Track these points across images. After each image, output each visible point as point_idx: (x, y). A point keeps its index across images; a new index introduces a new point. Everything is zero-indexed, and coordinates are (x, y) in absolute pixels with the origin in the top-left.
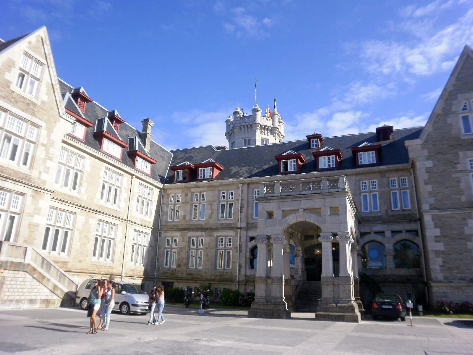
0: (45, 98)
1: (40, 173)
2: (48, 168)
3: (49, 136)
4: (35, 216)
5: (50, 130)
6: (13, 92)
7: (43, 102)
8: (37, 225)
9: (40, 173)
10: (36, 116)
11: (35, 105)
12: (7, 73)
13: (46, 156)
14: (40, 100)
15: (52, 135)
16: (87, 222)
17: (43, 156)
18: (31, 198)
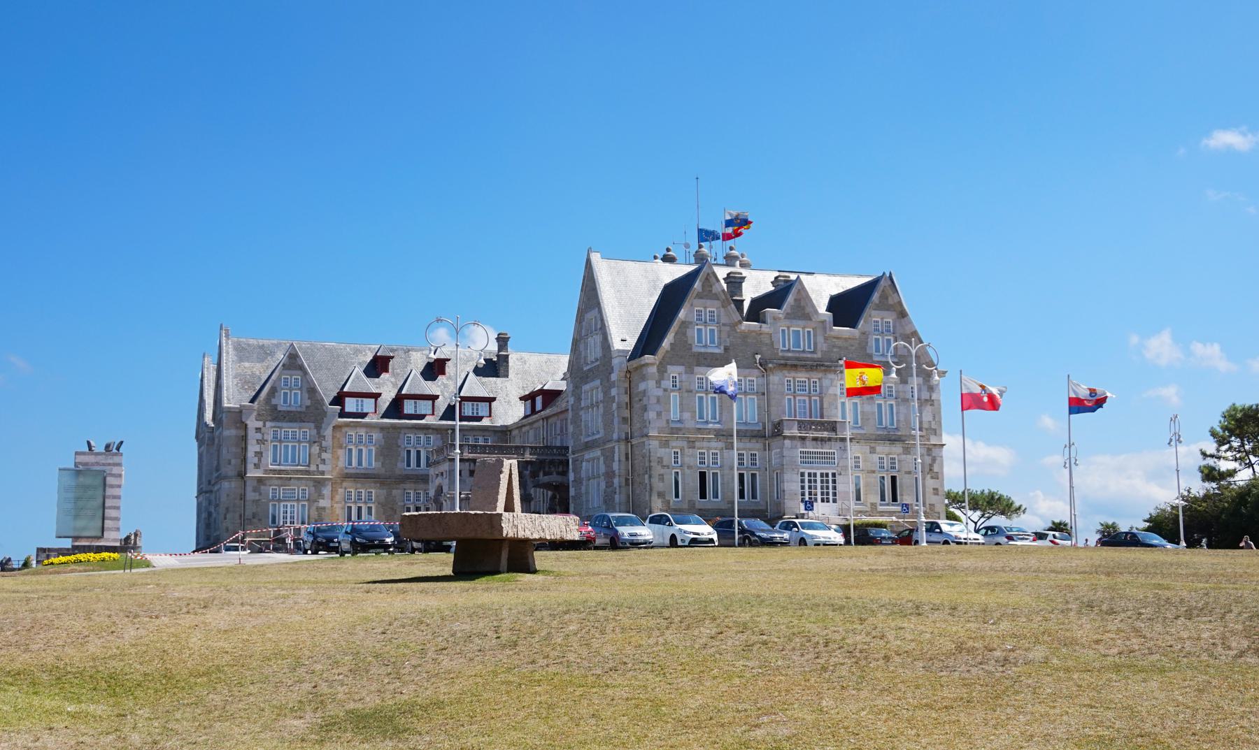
0: (308, 403)
1: (317, 465)
2: (324, 460)
3: (318, 433)
4: (321, 501)
5: (318, 428)
6: (280, 411)
7: (307, 407)
8: (324, 508)
9: (317, 465)
10: (304, 422)
11: (300, 412)
12: (273, 400)
13: (320, 449)
14: (304, 407)
15: (322, 431)
16: (389, 494)
17: (318, 451)
18: (313, 488)
